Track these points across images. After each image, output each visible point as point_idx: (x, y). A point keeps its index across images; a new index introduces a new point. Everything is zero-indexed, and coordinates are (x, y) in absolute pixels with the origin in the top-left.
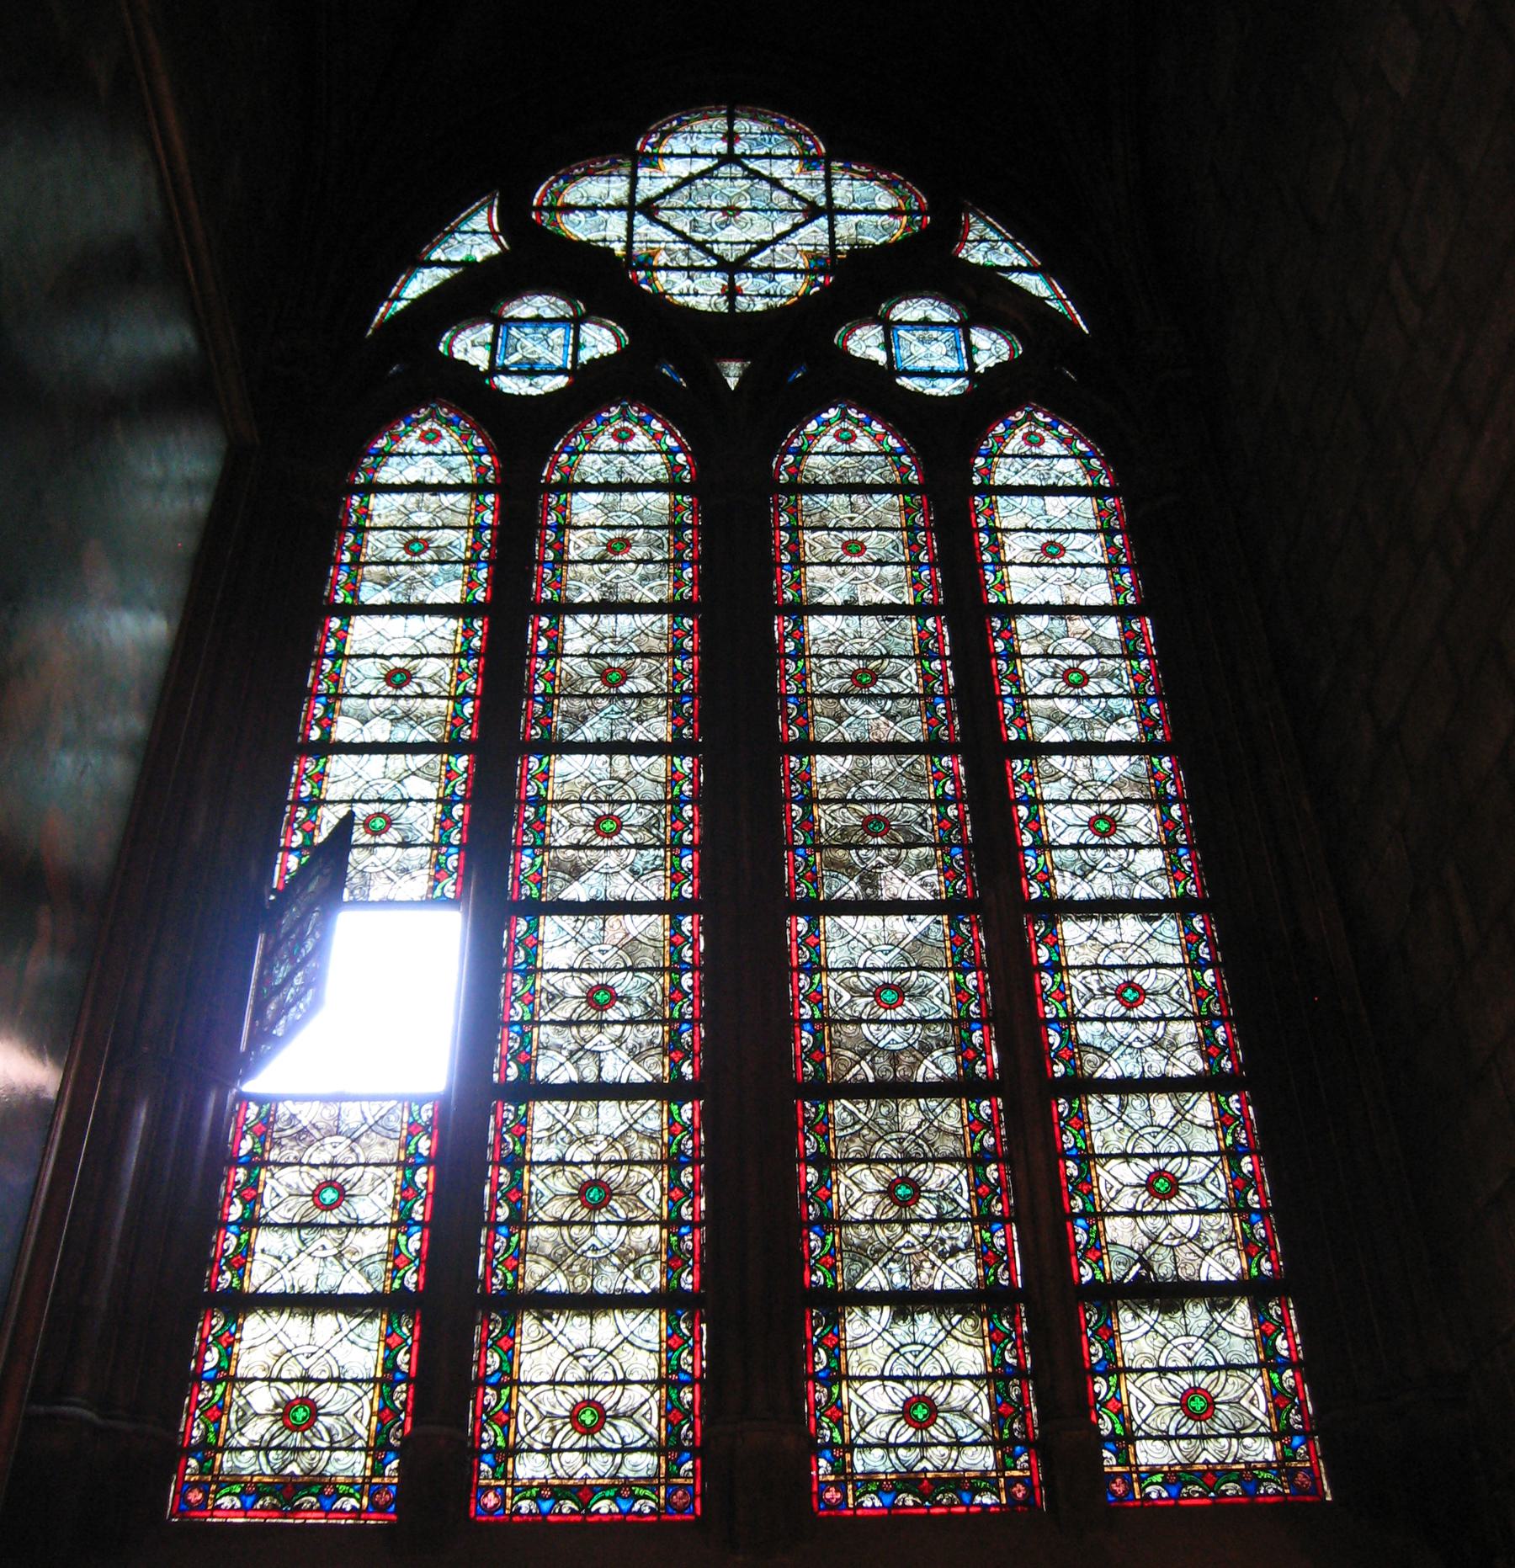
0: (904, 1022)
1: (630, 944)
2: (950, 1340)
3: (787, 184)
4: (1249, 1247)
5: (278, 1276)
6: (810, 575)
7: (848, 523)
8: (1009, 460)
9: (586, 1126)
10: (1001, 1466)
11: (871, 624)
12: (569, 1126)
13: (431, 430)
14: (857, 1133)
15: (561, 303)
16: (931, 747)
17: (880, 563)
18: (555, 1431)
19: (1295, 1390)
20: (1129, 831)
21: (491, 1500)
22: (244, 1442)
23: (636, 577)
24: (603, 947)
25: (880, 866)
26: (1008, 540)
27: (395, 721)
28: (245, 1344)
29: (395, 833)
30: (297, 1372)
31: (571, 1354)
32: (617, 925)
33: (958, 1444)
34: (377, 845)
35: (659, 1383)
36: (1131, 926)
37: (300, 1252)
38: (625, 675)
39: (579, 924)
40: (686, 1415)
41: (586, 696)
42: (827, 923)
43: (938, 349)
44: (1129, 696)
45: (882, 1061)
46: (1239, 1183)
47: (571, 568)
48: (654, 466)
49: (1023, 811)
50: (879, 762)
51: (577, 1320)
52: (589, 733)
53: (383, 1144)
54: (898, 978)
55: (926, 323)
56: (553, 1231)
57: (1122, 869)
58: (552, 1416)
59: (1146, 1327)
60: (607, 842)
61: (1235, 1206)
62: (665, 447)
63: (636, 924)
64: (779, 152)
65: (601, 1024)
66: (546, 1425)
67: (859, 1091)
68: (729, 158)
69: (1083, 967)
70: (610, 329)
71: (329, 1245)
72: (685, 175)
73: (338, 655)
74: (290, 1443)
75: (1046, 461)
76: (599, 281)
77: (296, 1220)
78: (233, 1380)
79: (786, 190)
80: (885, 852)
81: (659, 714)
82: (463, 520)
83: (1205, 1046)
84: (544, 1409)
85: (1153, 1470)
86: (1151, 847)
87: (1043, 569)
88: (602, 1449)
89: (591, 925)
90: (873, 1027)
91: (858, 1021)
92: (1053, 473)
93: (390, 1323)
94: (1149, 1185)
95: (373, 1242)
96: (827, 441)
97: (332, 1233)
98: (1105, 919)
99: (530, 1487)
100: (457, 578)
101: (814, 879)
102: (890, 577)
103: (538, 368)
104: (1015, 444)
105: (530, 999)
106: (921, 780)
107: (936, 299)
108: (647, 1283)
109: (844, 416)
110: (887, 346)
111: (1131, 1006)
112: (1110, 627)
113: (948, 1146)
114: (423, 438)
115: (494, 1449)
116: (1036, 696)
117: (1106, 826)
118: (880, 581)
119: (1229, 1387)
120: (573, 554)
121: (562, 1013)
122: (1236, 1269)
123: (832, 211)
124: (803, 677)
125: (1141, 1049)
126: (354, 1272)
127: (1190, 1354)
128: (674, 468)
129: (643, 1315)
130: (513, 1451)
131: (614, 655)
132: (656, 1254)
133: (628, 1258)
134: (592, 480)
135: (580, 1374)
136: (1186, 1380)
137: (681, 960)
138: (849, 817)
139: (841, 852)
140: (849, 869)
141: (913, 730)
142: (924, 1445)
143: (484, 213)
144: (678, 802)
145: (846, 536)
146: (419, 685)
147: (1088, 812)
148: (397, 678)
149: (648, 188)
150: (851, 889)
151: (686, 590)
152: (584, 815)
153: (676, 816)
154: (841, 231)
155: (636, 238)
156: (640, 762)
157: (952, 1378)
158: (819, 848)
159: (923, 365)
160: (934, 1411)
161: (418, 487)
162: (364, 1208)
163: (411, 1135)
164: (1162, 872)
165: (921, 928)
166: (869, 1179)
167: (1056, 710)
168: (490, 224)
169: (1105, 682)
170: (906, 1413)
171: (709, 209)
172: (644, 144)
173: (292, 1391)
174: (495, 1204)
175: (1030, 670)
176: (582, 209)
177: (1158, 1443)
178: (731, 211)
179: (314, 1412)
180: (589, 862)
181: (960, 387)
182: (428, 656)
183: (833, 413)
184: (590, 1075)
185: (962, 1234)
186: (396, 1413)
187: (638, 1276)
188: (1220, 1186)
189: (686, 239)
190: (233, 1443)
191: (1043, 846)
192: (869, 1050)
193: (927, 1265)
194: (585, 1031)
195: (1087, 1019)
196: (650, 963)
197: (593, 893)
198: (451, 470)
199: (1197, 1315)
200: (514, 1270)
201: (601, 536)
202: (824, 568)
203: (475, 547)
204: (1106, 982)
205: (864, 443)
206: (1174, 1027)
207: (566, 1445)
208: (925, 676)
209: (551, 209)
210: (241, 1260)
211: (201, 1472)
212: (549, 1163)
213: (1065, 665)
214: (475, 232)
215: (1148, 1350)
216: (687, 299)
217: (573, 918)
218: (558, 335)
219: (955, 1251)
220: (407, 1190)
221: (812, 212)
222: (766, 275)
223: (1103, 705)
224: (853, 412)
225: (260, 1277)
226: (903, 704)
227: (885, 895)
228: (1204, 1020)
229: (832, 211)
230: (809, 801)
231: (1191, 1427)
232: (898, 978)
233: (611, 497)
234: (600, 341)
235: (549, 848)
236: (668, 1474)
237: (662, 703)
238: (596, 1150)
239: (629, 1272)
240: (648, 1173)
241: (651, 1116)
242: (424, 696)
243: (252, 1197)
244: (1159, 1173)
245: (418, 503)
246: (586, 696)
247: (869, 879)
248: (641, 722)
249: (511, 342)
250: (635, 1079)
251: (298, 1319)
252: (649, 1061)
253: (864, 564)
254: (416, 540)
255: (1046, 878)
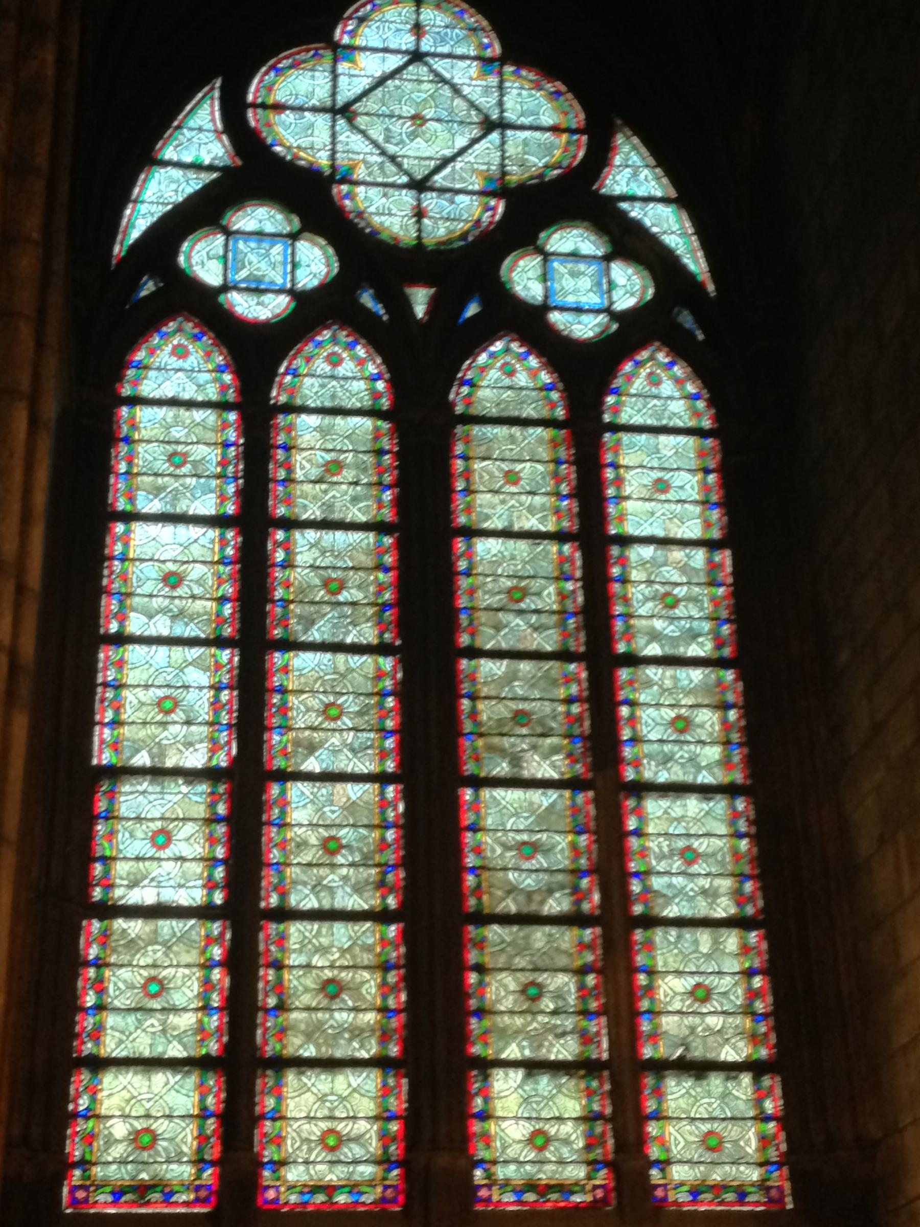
0: (537, 871)
1: (351, 807)
2: (560, 1095)
3: (466, 90)
4: (754, 1039)
5: (123, 1046)
6: (478, 502)
7: (508, 455)
8: (634, 399)
9: (324, 941)
10: (589, 1178)
11: (522, 546)
12: (314, 941)
13: (179, 345)
14: (502, 950)
15: (279, 217)
16: (563, 656)
17: (532, 493)
18: (310, 1151)
19: (775, 1136)
20: (699, 730)
21: (271, 1194)
22: (110, 1159)
23: (347, 497)
24: (333, 808)
25: (523, 751)
26: (628, 476)
27: (174, 618)
28: (105, 1093)
29: (181, 713)
30: (141, 1112)
31: (319, 1099)
32: (341, 792)
33: (561, 1162)
34: (166, 723)
35: (376, 1118)
36: (693, 805)
37: (137, 1028)
38: (342, 586)
39: (315, 790)
40: (393, 1139)
41: (312, 603)
42: (486, 793)
43: (585, 283)
44: (710, 618)
45: (521, 898)
46: (752, 995)
47: (298, 487)
48: (357, 392)
49: (624, 711)
50: (525, 666)
51: (323, 1077)
52: (315, 635)
53: (188, 952)
54: (536, 837)
55: (575, 256)
56: (304, 1015)
57: (691, 760)
58: (308, 1141)
59: (684, 1091)
60: (332, 725)
61: (748, 1011)
62: (367, 374)
63: (355, 791)
64: (459, 51)
65: (333, 866)
66: (305, 1147)
67: (506, 919)
68: (417, 56)
69: (659, 835)
70: (321, 248)
71: (156, 1023)
72: (378, 74)
73: (124, 559)
74: (140, 1159)
75: (662, 401)
76: (311, 198)
77: (133, 1005)
78: (98, 1117)
79: (464, 97)
80: (527, 740)
81: (367, 621)
82: (211, 436)
83: (739, 898)
84: (304, 1135)
85: (682, 1184)
86: (712, 743)
87: (653, 504)
88: (339, 1162)
89: (324, 791)
90: (516, 875)
91: (505, 869)
92: (666, 414)
93: (201, 1077)
94: (692, 993)
95: (187, 1020)
96: (494, 374)
97: (158, 1015)
98: (678, 797)
99: (295, 1187)
100: (211, 492)
101: (477, 759)
102: (538, 506)
103: (263, 287)
104: (639, 384)
105: (282, 845)
106: (554, 683)
107: (587, 229)
108: (368, 1051)
109: (507, 350)
110: (545, 278)
111: (690, 863)
112: (699, 557)
113: (563, 961)
114: (173, 353)
115: (271, 1162)
116: (640, 616)
117: (682, 725)
118: (531, 510)
119: (732, 1131)
120: (299, 474)
121: (306, 858)
122: (744, 1055)
123: (503, 125)
124: (471, 592)
125: (693, 897)
126: (175, 1043)
127: (710, 1109)
128: (376, 395)
129: (364, 1075)
130: (283, 1163)
131: (334, 568)
132: (373, 1031)
133: (356, 1032)
134: (311, 403)
135: (326, 1112)
136: (705, 1127)
137: (385, 820)
138: (503, 710)
139: (496, 740)
140: (502, 752)
141: (548, 642)
142: (542, 1162)
143: (206, 106)
144: (383, 694)
145: (505, 466)
146: (189, 586)
147: (672, 714)
148: (172, 580)
149: (349, 88)
150: (502, 768)
151: (385, 511)
152: (314, 703)
153: (381, 706)
154: (511, 150)
155: (339, 147)
156: (356, 661)
157: (560, 1119)
158: (481, 735)
159: (571, 300)
160: (548, 1140)
161: (174, 402)
162: (178, 998)
163: (207, 946)
164: (719, 763)
165: (551, 801)
166: (511, 982)
167: (653, 628)
168: (213, 120)
169: (691, 606)
170: (530, 1141)
171: (400, 117)
172: (343, 32)
173: (138, 1125)
174: (266, 995)
175: (637, 592)
176: (293, 109)
177: (686, 1167)
178: (418, 119)
179: (155, 1138)
180: (320, 741)
181: (598, 325)
182: (194, 561)
183: (498, 346)
184: (326, 904)
185: (569, 1023)
186: (207, 1138)
187: (362, 1046)
188: (738, 997)
189: (383, 153)
190: (103, 1160)
191: (635, 740)
192: (512, 890)
193: (546, 1044)
194: (322, 871)
195: (659, 873)
196: (365, 822)
197: (324, 766)
198: (199, 386)
199: (716, 1081)
200: (280, 1040)
201: (322, 457)
202: (489, 496)
203: (224, 463)
204: (674, 845)
205: (522, 379)
206: (718, 882)
207: (319, 1159)
208: (562, 596)
209: (264, 106)
210: (97, 1034)
211: (83, 1178)
212: (300, 967)
213: (662, 589)
214: (200, 129)
215: (684, 1106)
216: (383, 218)
217: (311, 784)
218: (277, 250)
219: (564, 1034)
220: (207, 984)
221: (489, 125)
222: (448, 195)
223: (688, 626)
224: (515, 346)
225: (110, 1047)
226: (544, 619)
227: (526, 774)
228: (741, 877)
229: (503, 125)
230: (473, 697)
231: (708, 1157)
232: (536, 837)
233: (328, 420)
234: (315, 263)
235: (290, 729)
236: (384, 1179)
237: (370, 611)
238: (332, 958)
239: (356, 1045)
240: (366, 975)
241: (367, 932)
242: (194, 597)
243: (100, 987)
244: (698, 986)
245: (176, 417)
246: (312, 603)
247: (516, 760)
248: (355, 624)
249: (240, 256)
250: (357, 907)
251: (140, 1077)
252: (366, 894)
253: (521, 493)
254: (175, 454)
255: (637, 763)
